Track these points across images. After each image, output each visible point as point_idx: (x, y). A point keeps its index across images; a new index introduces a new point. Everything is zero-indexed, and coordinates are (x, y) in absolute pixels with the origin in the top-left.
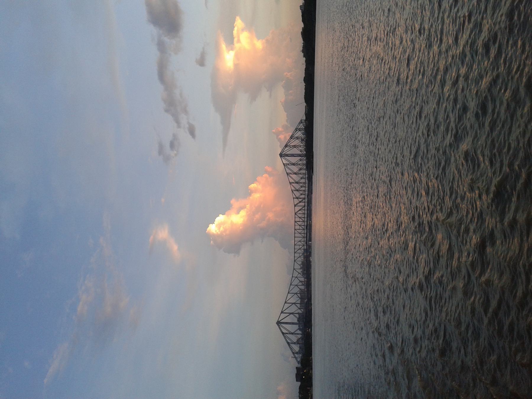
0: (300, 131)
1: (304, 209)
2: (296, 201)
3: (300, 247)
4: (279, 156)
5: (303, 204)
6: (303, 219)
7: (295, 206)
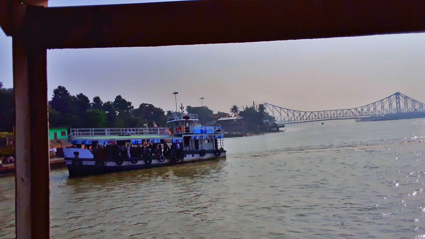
2: (359, 109)
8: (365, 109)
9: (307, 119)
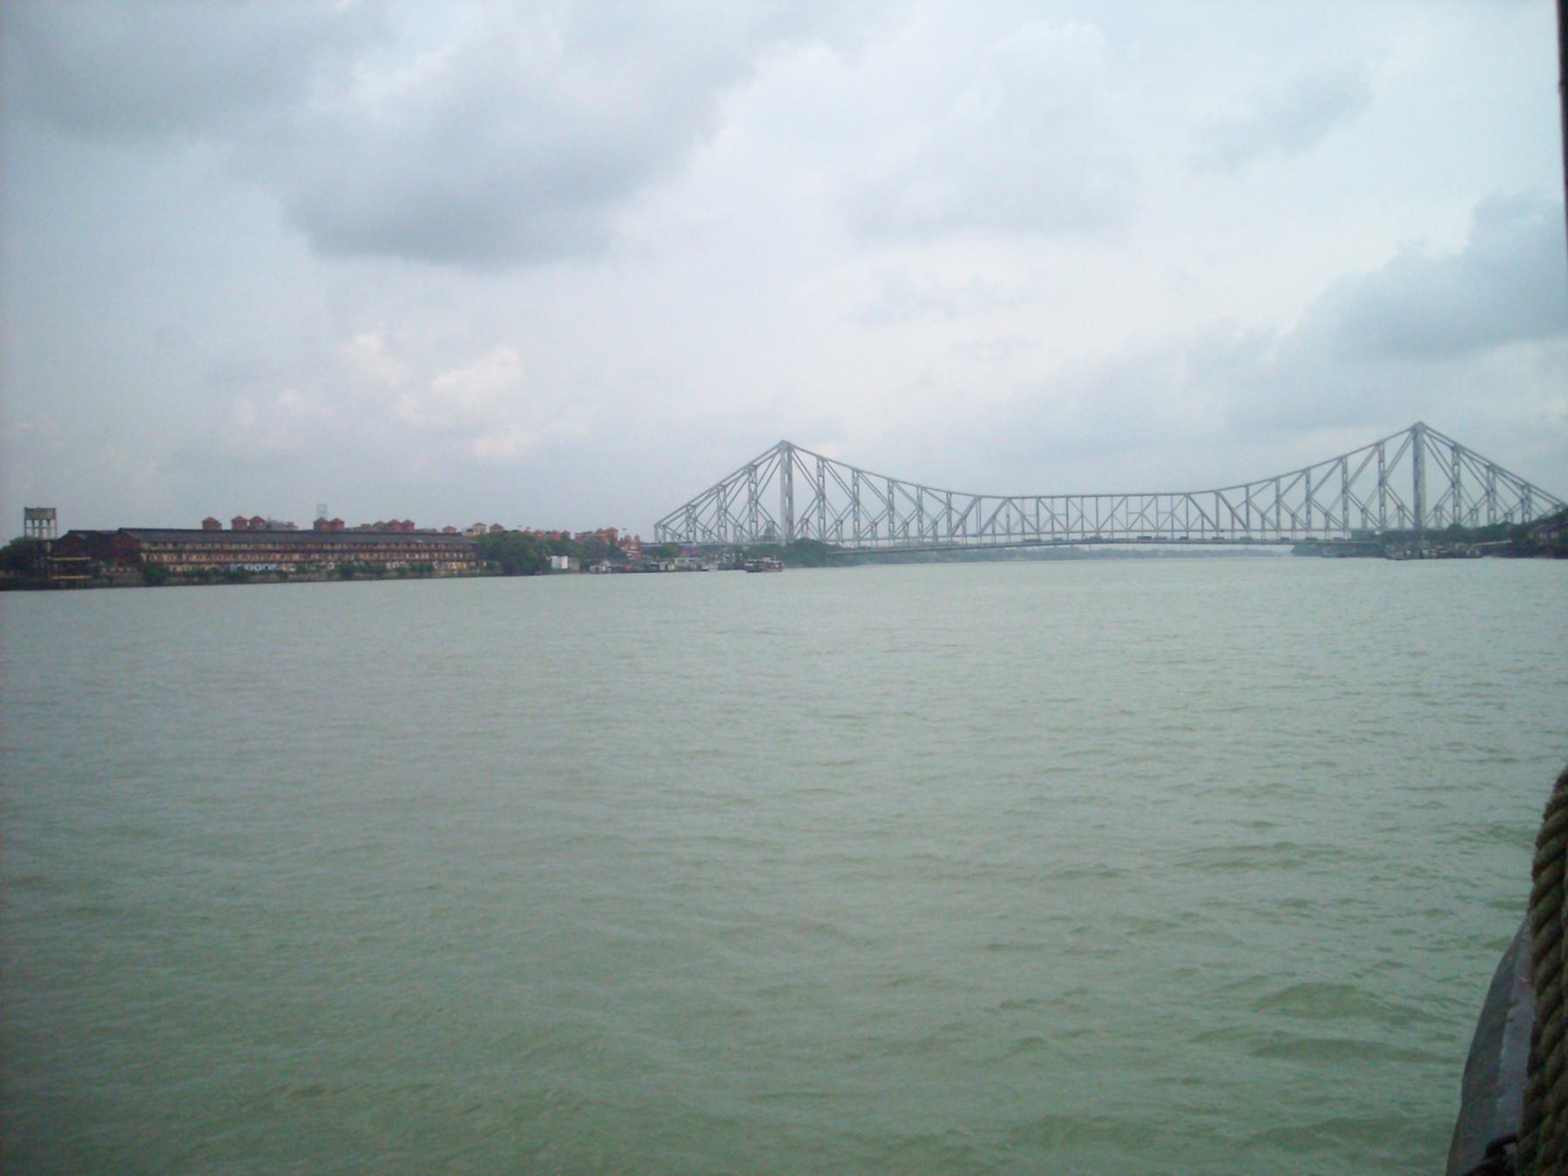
0: (1522, 501)
2: (1236, 498)
4: (1417, 420)
5: (1225, 522)
9: (981, 534)
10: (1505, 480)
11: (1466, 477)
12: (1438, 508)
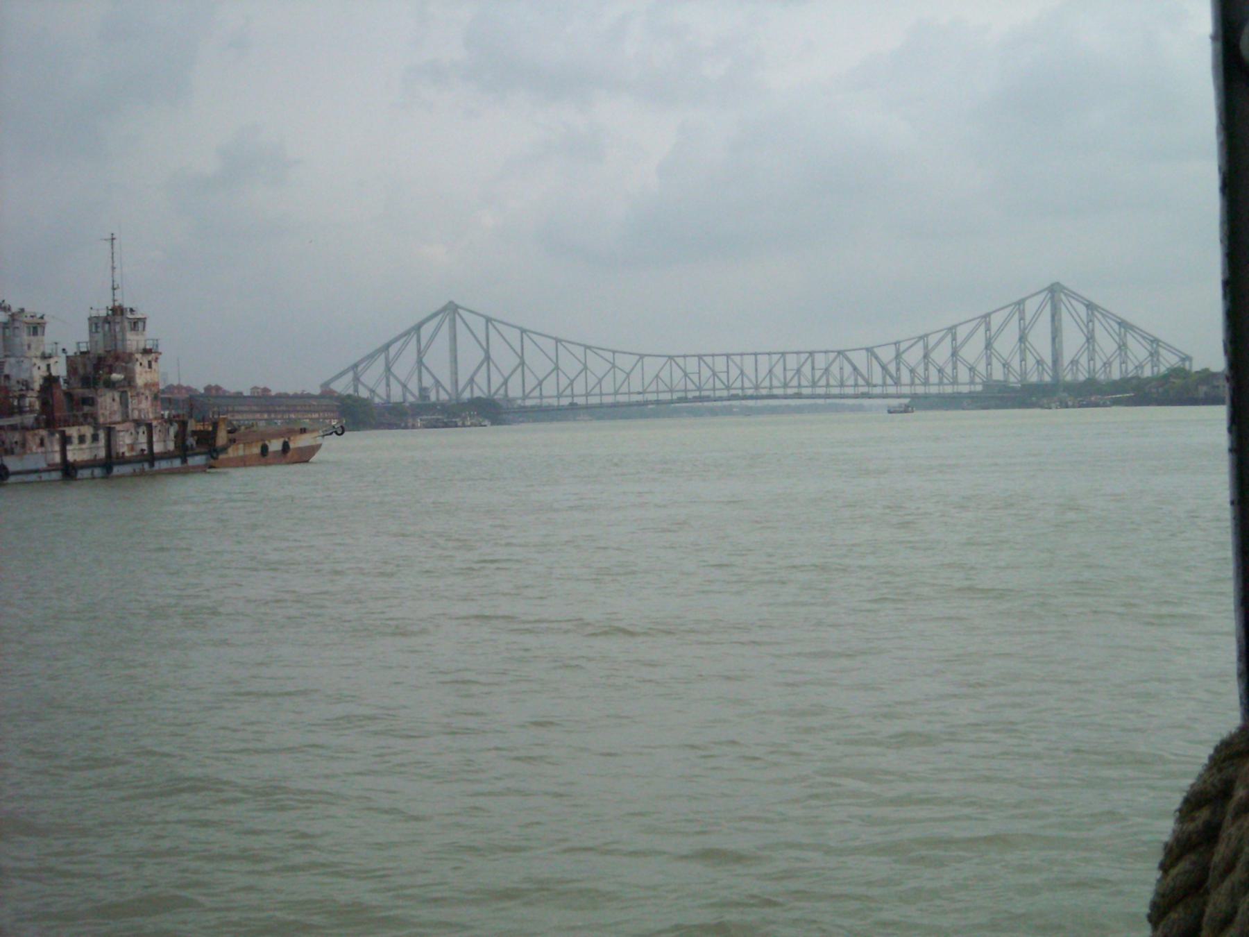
0: (1151, 355)
1: (861, 382)
2: (887, 354)
3: (720, 375)
5: (877, 377)
6: (823, 382)
7: (869, 350)
8: (914, 356)
10: (1136, 335)
11: (1100, 333)
12: (1074, 362)
